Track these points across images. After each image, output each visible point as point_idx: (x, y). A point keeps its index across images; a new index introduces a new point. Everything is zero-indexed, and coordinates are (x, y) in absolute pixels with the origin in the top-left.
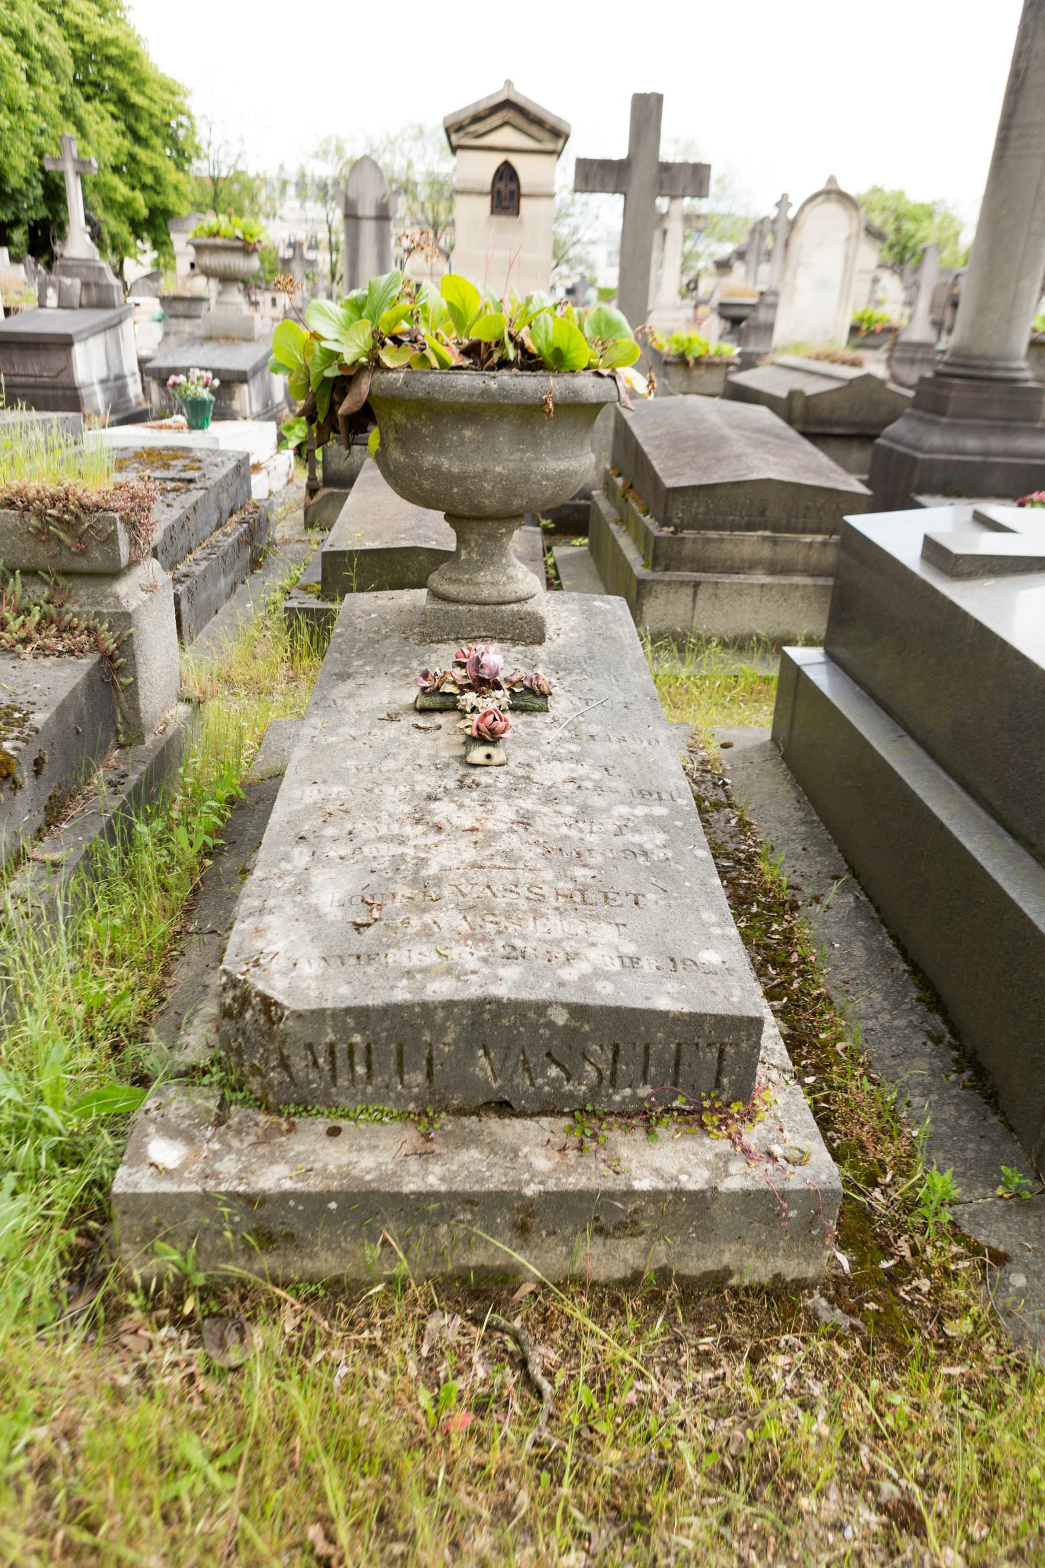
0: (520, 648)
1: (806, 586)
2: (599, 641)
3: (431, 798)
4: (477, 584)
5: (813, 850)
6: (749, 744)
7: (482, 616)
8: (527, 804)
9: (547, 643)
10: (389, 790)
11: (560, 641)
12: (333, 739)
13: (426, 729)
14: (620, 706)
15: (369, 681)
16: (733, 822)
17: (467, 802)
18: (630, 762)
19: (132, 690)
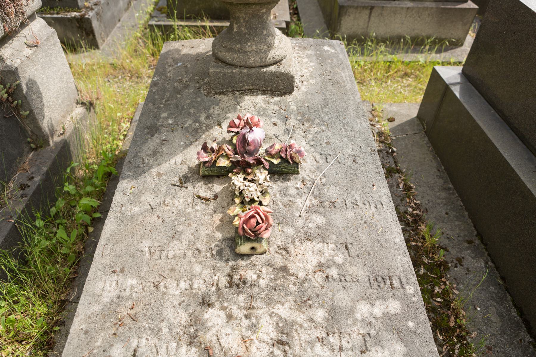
0: (277, 99)
1: (432, 8)
2: (330, 87)
3: (206, 303)
4: (245, 52)
5: (452, 214)
6: (404, 120)
7: (250, 76)
8: (285, 310)
9: (296, 92)
10: (172, 286)
11: (304, 89)
12: (136, 209)
13: (207, 200)
14: (350, 161)
15: (170, 136)
16: (401, 186)
17: (236, 312)
18: (363, 235)
19: (33, 119)
